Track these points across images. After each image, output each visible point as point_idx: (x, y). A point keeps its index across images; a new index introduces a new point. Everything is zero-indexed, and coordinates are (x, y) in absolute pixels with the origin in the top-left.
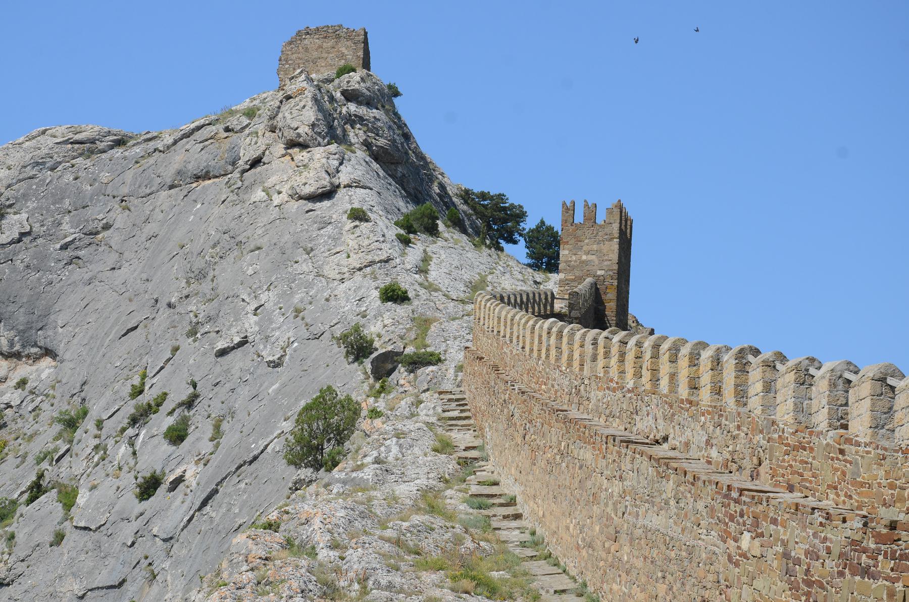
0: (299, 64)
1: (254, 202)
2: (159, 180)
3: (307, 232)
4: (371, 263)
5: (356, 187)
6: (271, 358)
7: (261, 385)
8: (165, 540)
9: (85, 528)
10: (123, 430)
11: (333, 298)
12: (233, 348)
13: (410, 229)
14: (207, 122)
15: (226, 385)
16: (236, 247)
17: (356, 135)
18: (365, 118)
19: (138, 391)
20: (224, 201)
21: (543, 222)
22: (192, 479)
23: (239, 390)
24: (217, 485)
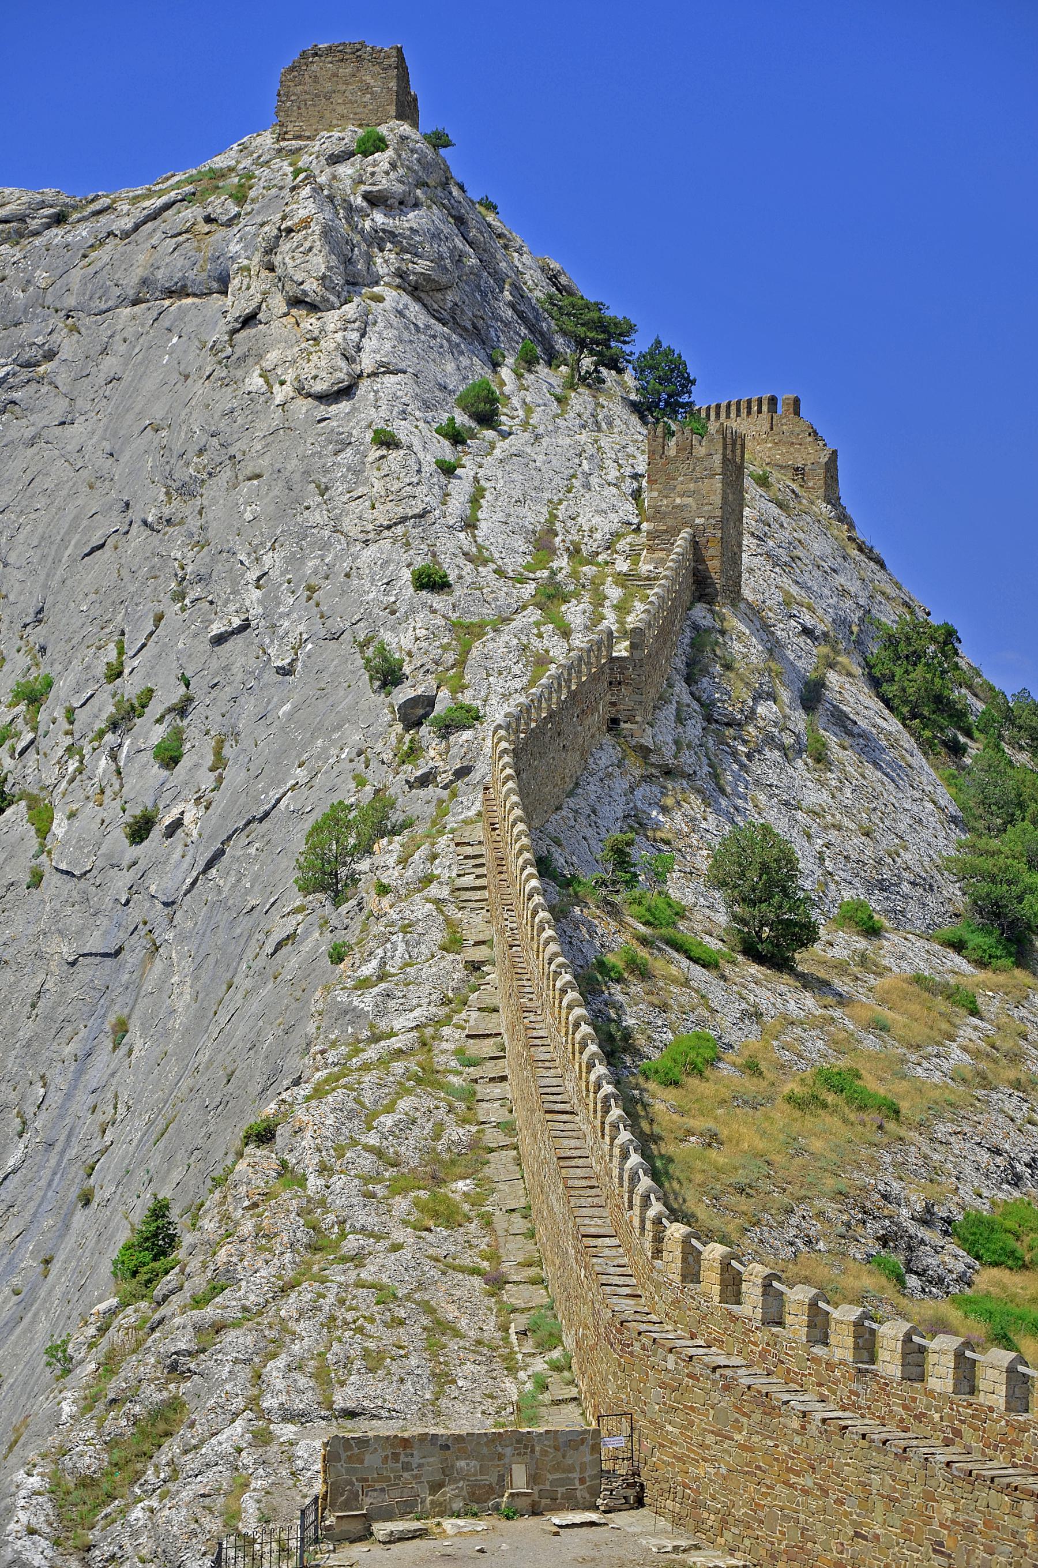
0: (305, 101)
1: (249, 393)
2: (117, 291)
3: (320, 458)
4: (404, 519)
5: (383, 373)
6: (279, 663)
7: (268, 703)
8: (166, 904)
9: (67, 873)
10: (101, 734)
11: (354, 572)
12: (232, 633)
13: (457, 438)
14: (180, 197)
15: (226, 689)
16: (228, 462)
17: (385, 262)
18: (397, 232)
19: (115, 673)
20: (210, 375)
21: (658, 343)
22: (192, 826)
23: (242, 700)
24: (222, 843)
